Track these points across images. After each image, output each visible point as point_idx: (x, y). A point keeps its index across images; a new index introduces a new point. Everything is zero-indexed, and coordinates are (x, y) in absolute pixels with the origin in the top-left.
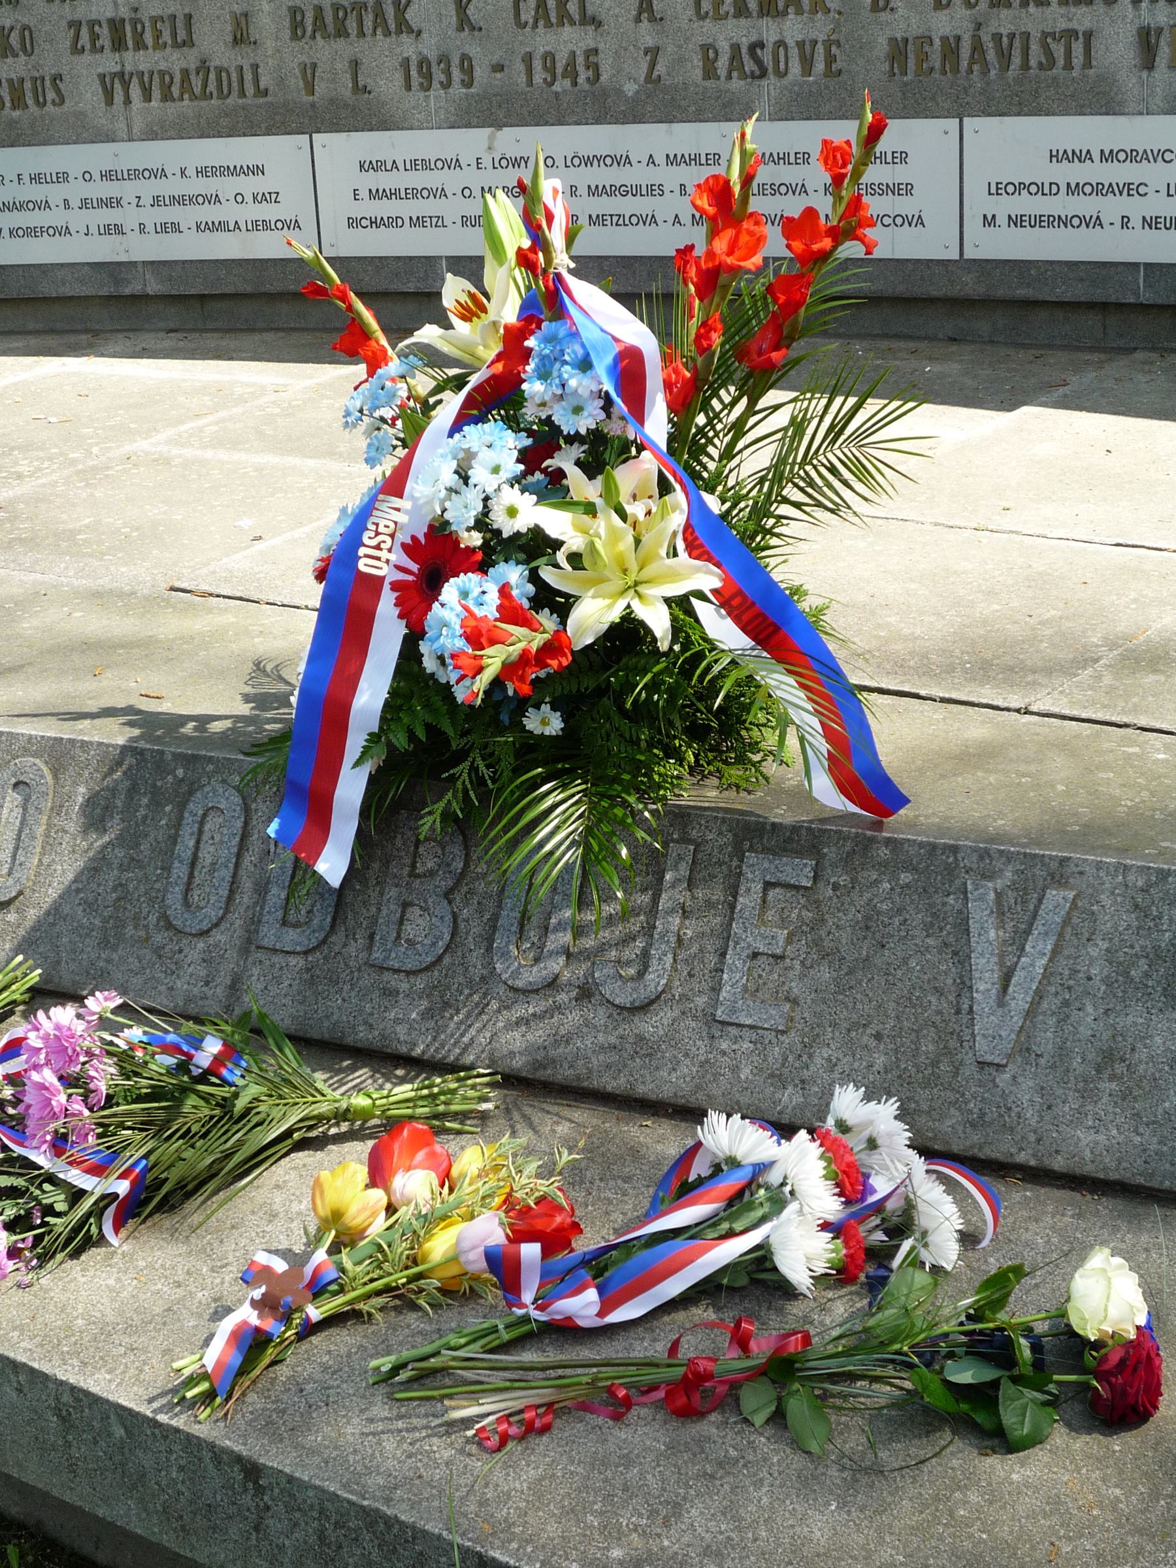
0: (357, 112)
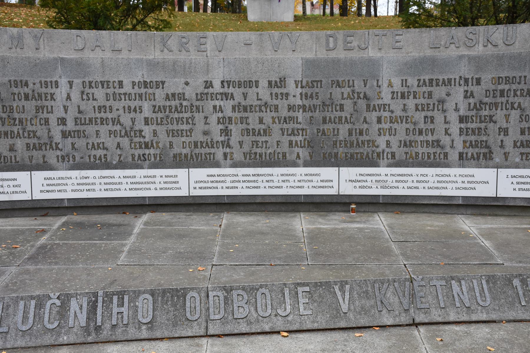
0: (45, 166)
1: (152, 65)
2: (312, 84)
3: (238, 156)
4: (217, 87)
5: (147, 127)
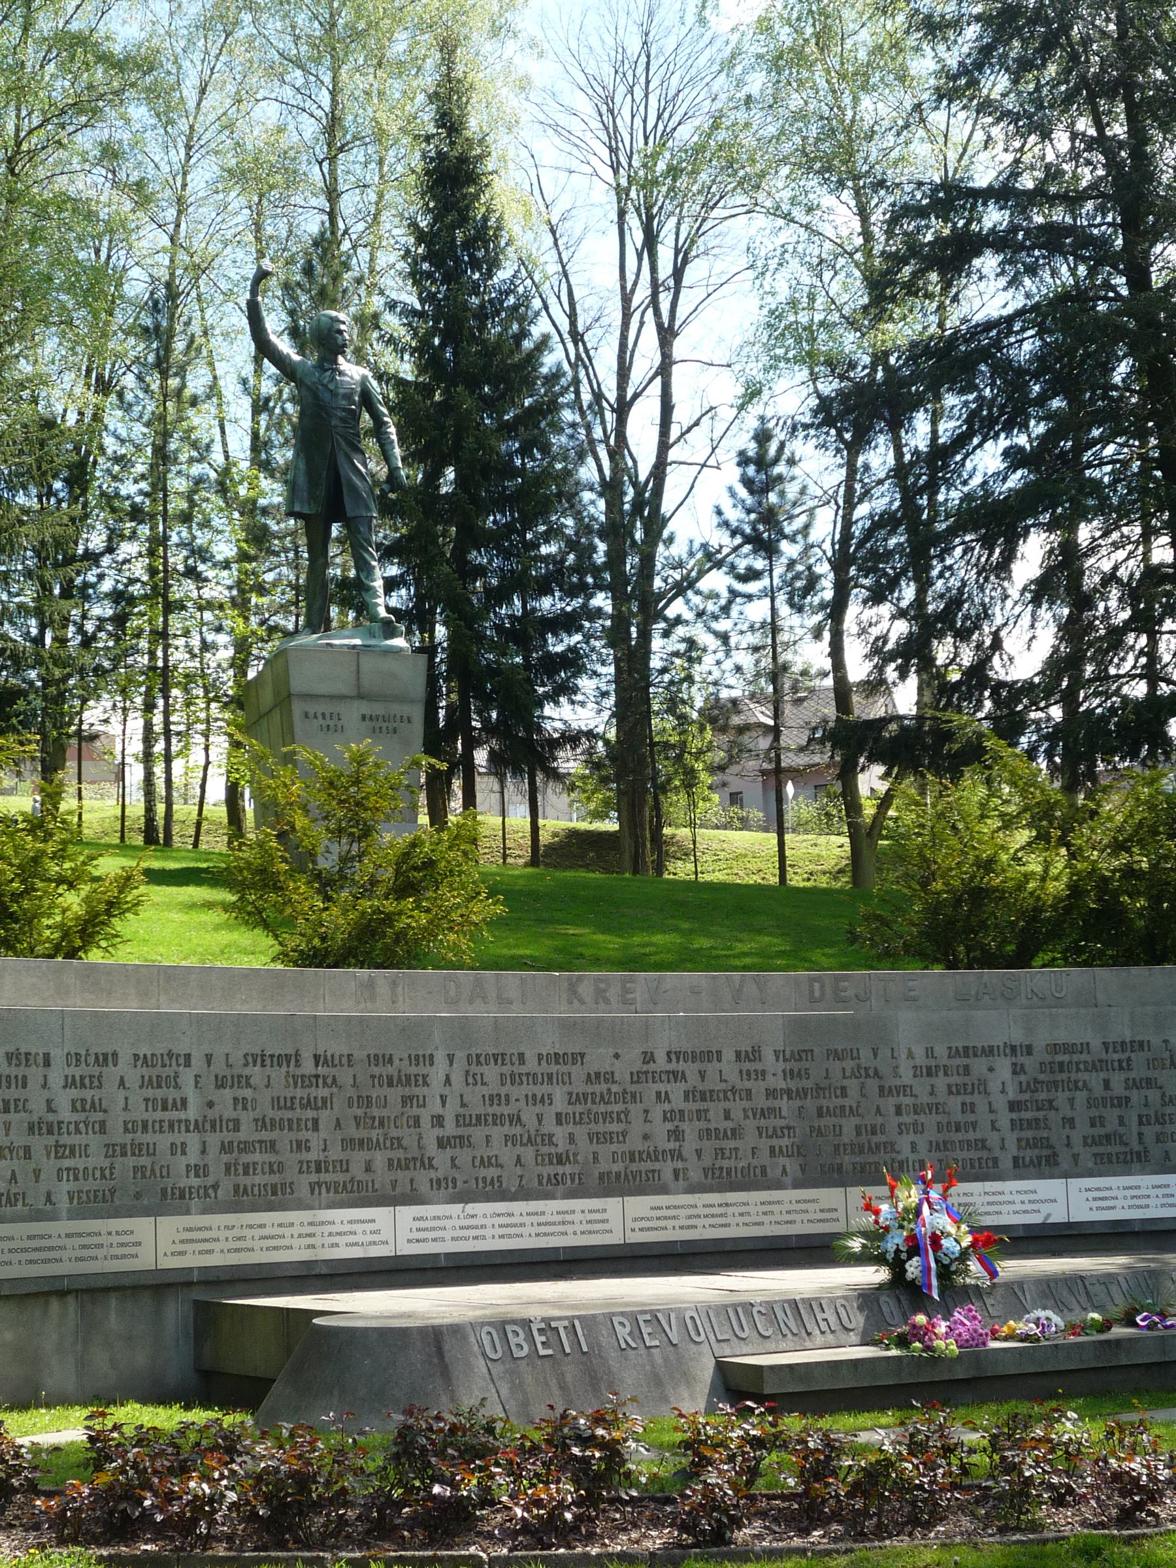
0: (412, 1198)
1: (567, 1026)
2: (798, 1056)
3: (695, 1175)
4: (661, 1063)
5: (560, 1128)
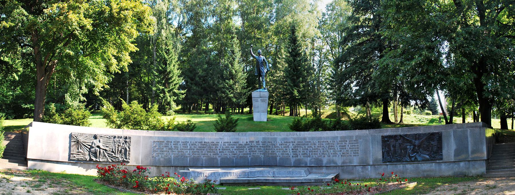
2: (264, 142)
